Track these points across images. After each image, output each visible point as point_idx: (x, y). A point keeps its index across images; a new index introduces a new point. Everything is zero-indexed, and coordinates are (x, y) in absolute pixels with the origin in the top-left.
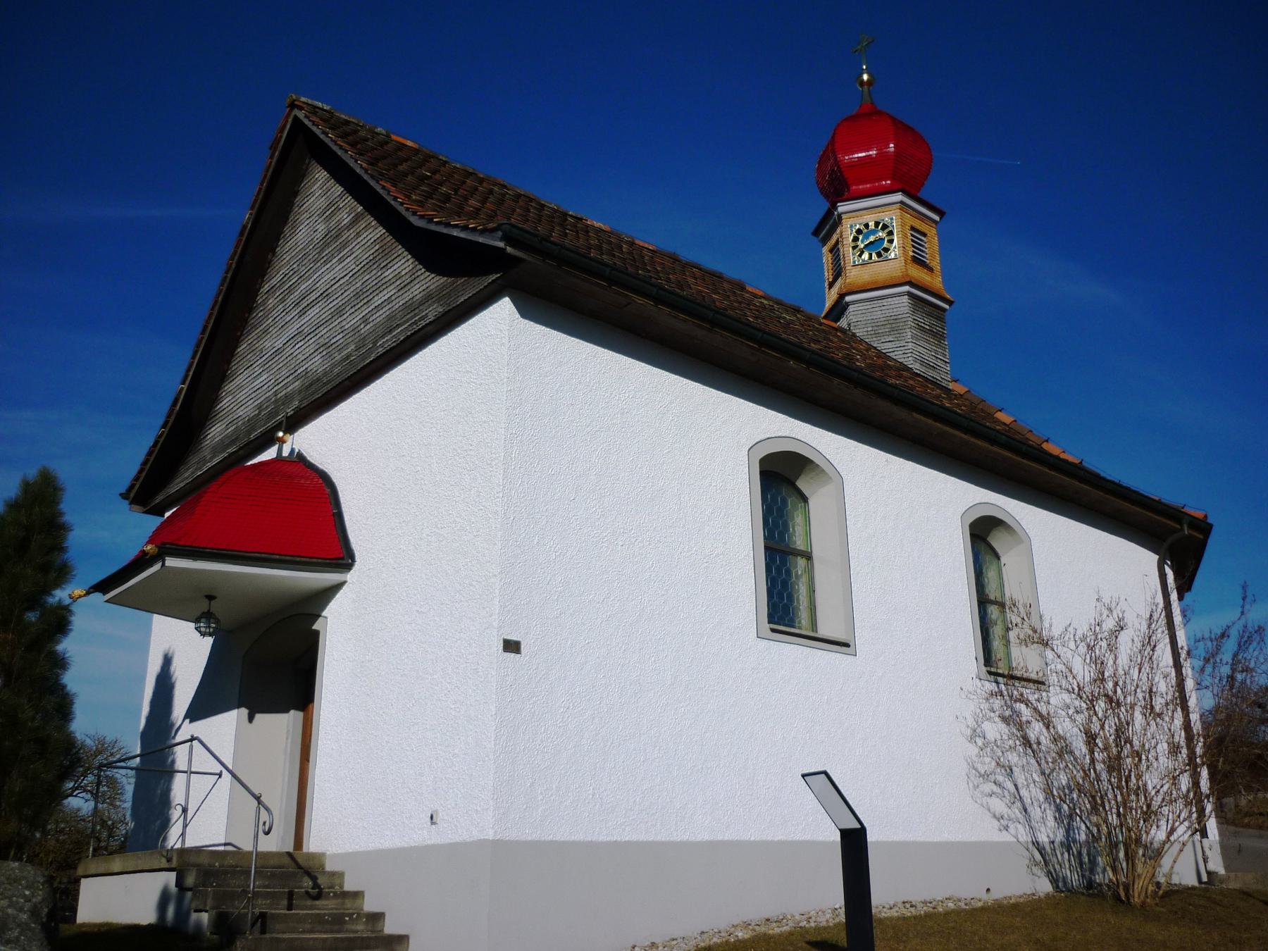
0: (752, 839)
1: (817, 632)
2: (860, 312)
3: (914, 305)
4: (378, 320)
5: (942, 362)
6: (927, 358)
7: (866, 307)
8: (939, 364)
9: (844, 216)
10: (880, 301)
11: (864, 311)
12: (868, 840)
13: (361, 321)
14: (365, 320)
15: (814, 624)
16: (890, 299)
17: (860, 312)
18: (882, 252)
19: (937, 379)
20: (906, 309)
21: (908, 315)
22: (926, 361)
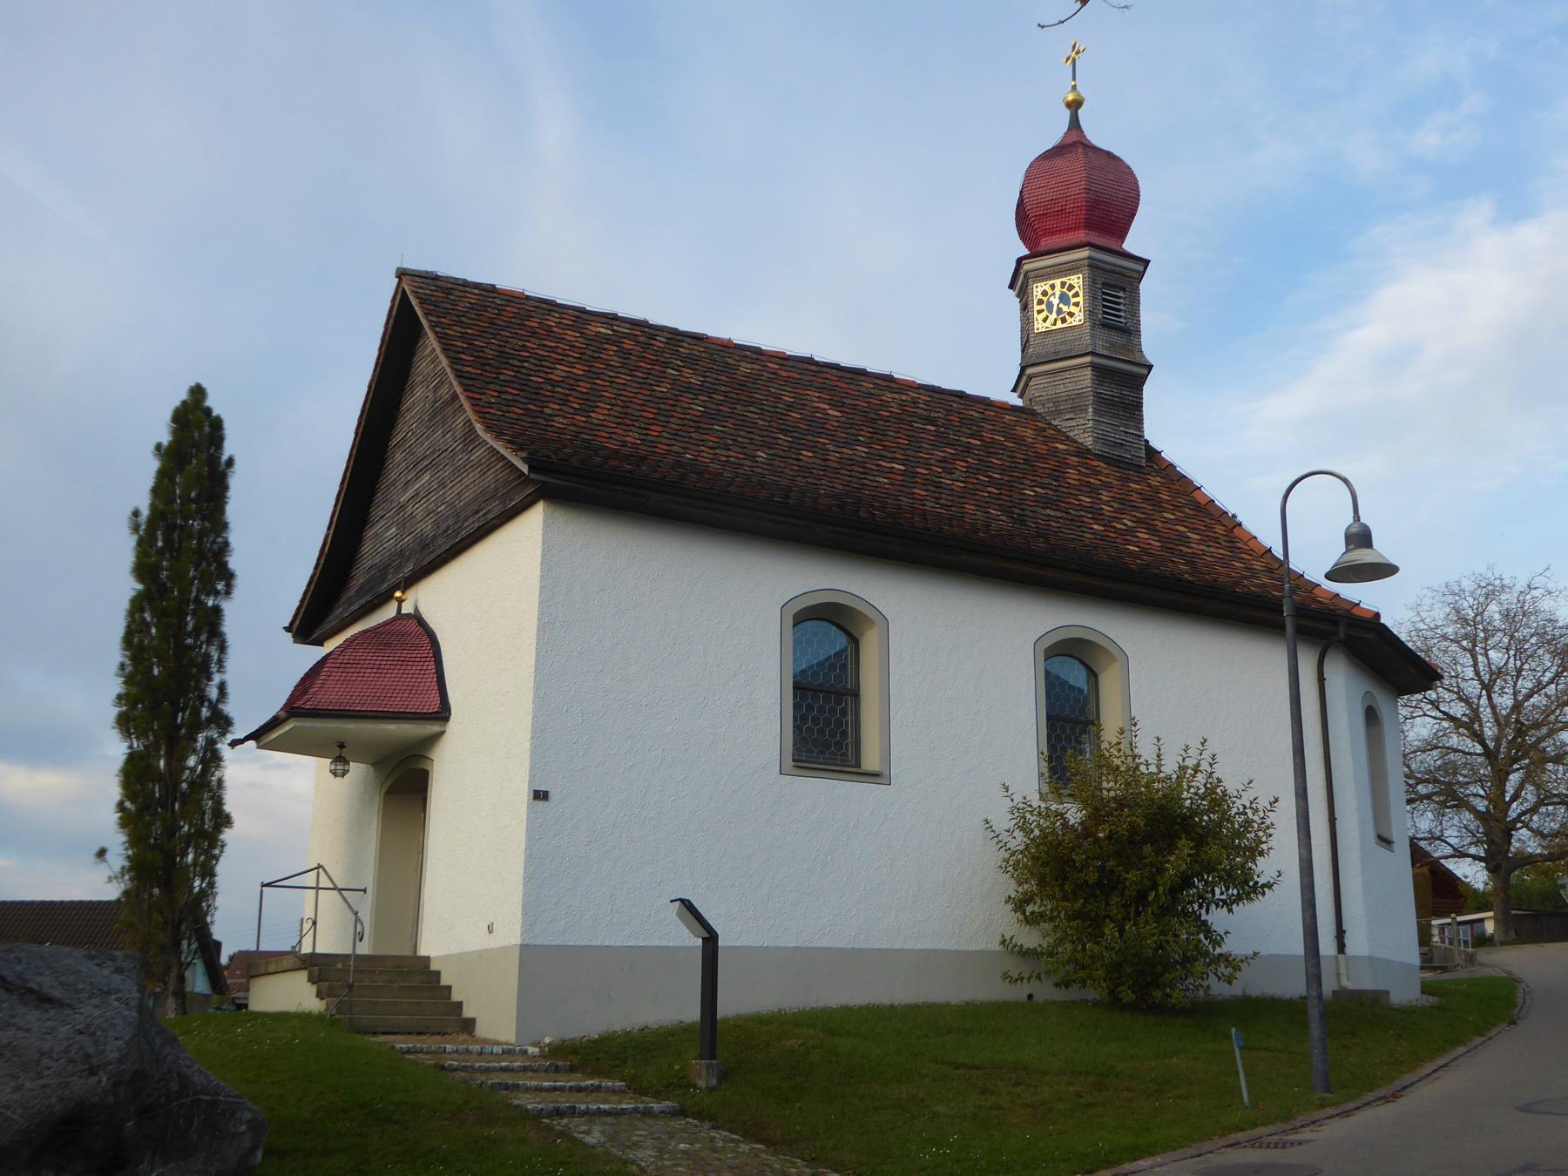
0: (765, 945)
1: (860, 767)
2: (1042, 386)
3: (1100, 377)
4: (467, 499)
5: (1134, 437)
6: (1113, 435)
7: (1048, 380)
8: (1130, 440)
9: (1031, 275)
10: (1063, 374)
11: (1046, 385)
12: (719, 944)
13: (456, 498)
14: (460, 494)
15: (858, 765)
16: (1073, 372)
17: (1042, 386)
18: (1067, 317)
19: (1124, 457)
20: (1088, 382)
21: (1090, 389)
22: (1110, 439)
